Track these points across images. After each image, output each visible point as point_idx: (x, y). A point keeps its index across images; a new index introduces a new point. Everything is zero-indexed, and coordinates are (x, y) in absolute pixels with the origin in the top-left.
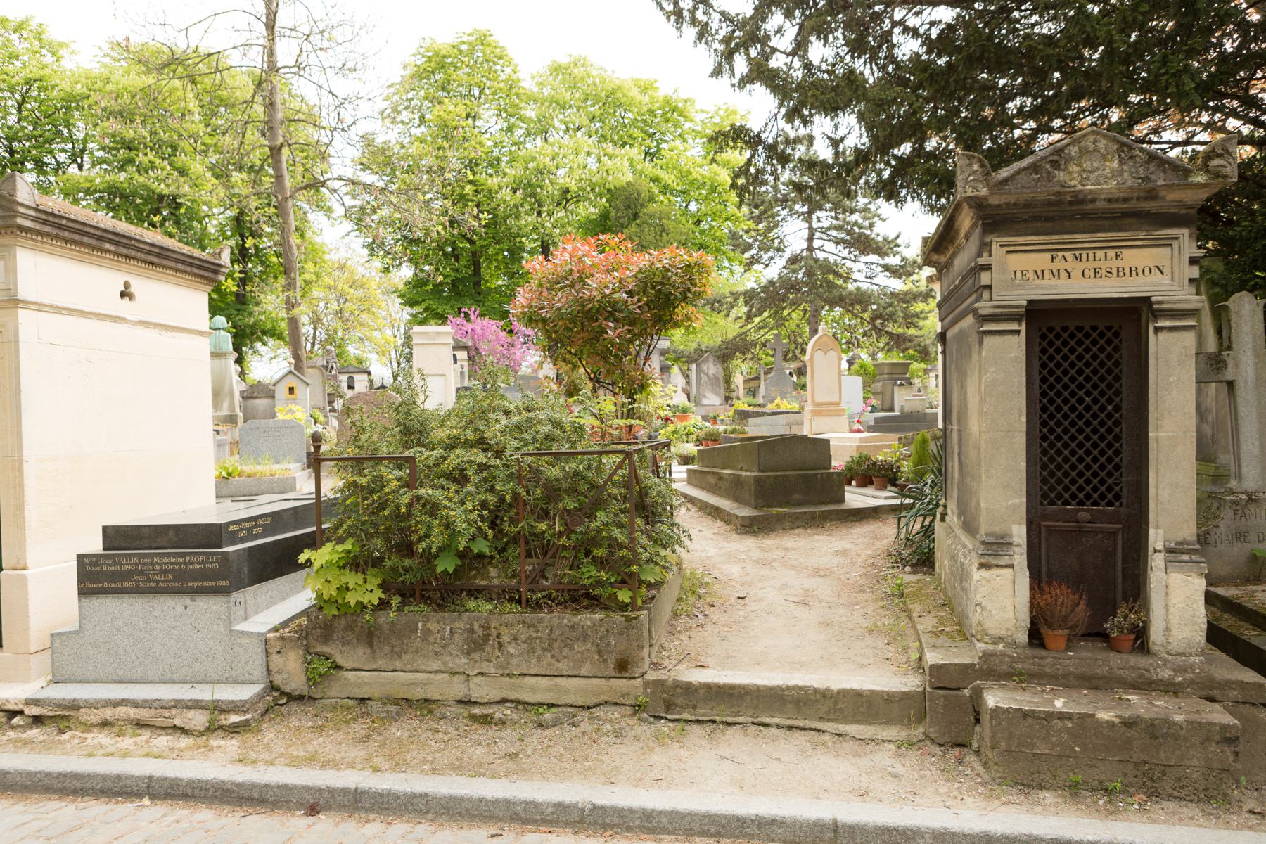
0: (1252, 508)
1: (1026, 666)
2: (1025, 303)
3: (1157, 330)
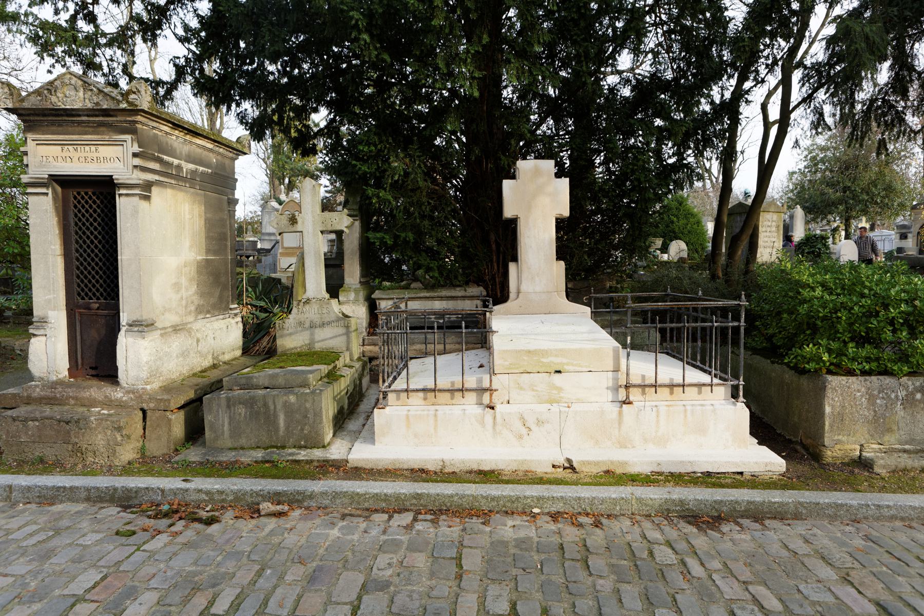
0: (307, 307)
3: (120, 195)
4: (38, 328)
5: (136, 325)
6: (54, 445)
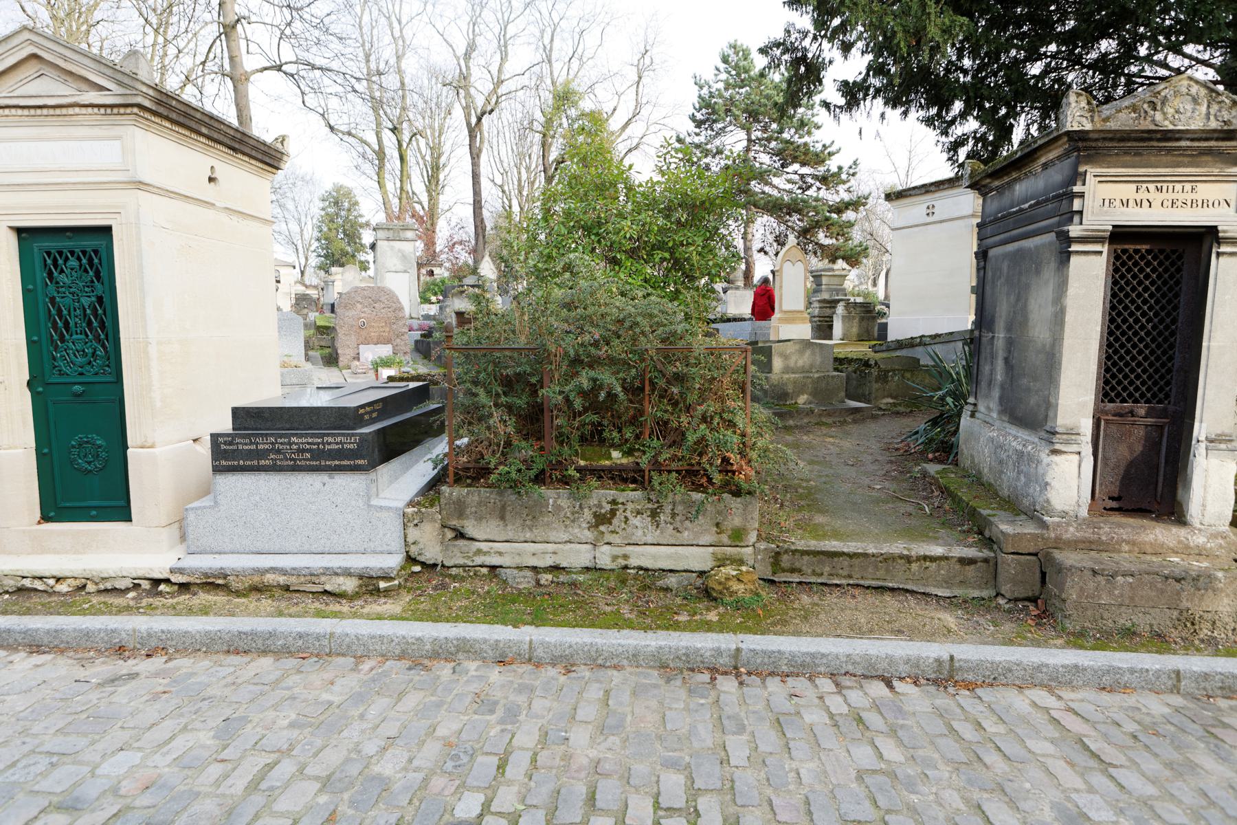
1: (1087, 535)
2: (1110, 228)
4: (1067, 443)
5: (1220, 442)
6: (1151, 611)
